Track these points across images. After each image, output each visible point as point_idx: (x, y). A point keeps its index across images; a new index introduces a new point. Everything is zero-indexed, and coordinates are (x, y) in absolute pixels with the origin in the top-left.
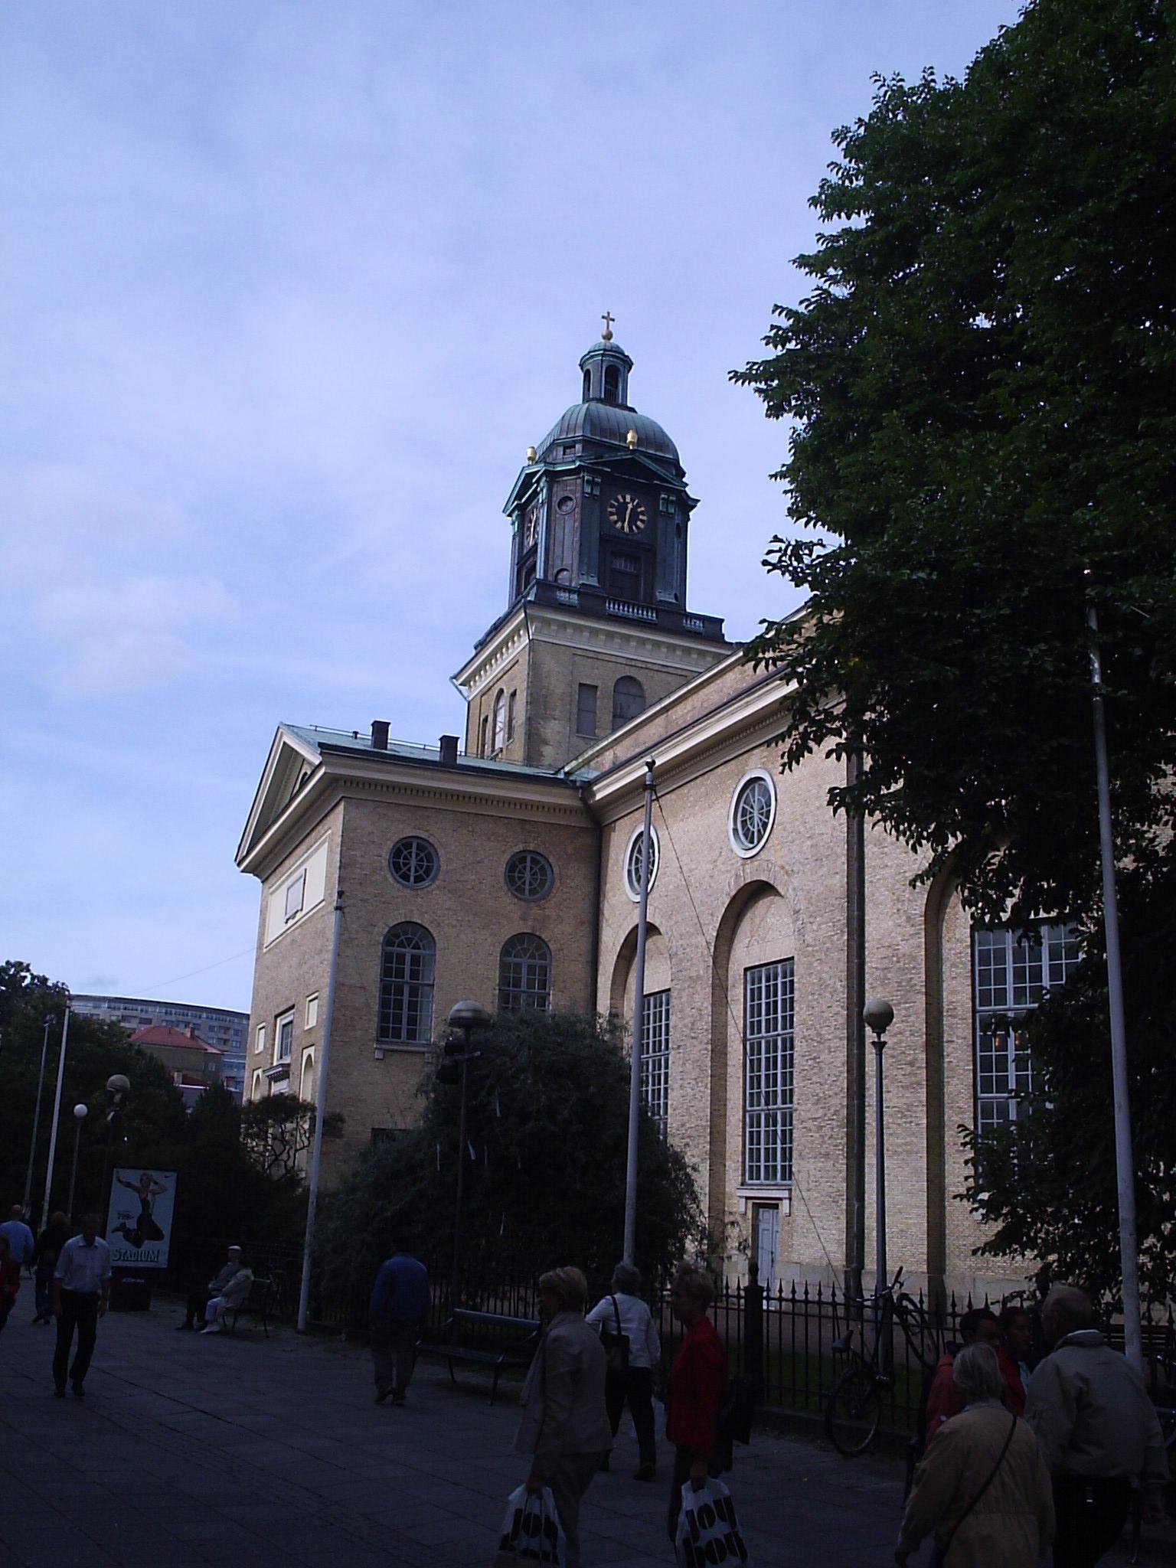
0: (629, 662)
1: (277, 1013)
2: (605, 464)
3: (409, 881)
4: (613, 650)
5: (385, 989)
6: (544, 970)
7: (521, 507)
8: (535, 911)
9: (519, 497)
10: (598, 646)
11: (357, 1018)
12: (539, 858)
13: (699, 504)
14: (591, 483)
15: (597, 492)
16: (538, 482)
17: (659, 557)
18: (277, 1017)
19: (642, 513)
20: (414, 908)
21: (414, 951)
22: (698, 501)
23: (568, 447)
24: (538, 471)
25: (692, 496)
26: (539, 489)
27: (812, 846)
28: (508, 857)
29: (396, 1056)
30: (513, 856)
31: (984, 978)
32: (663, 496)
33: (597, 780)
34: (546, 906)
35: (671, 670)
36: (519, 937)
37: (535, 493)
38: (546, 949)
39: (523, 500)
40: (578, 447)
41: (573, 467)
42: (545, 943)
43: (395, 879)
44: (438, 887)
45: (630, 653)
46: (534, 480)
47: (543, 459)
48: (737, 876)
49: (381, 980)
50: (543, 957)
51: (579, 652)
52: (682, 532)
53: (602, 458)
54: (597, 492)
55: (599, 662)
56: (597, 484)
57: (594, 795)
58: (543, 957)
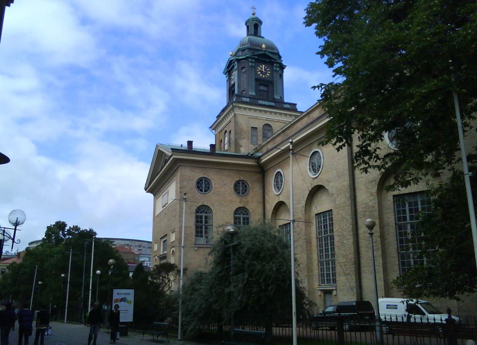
1: (161, 237)
2: (256, 55)
5: (197, 227)
6: (248, 219)
7: (229, 71)
8: (244, 200)
9: (228, 68)
10: (257, 114)
13: (286, 67)
15: (253, 65)
16: (234, 63)
17: (275, 84)
19: (268, 71)
21: (205, 214)
22: (286, 66)
23: (243, 50)
28: (234, 182)
29: (202, 249)
30: (235, 182)
31: (399, 212)
32: (275, 65)
34: (248, 197)
36: (239, 208)
37: (233, 67)
41: (245, 57)
42: (248, 210)
43: (198, 191)
44: (212, 193)
47: (235, 55)
48: (311, 184)
52: (281, 76)
53: (254, 53)
54: (253, 65)
56: (253, 62)
57: (261, 160)
58: (247, 214)
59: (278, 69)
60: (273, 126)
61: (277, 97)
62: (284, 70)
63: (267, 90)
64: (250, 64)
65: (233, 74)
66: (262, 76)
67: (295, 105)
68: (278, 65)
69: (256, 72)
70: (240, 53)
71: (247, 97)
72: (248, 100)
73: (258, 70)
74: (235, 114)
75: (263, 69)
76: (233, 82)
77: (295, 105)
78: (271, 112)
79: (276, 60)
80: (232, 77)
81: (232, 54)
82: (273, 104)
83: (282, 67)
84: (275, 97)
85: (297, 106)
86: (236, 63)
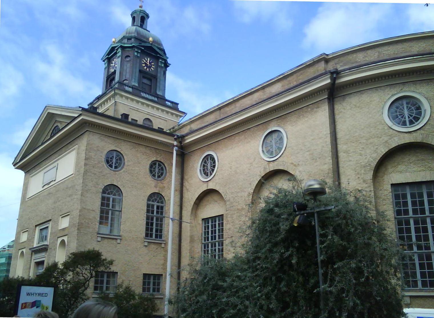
1: (36, 224)
3: (112, 168)
5: (102, 212)
6: (162, 208)
7: (109, 58)
9: (108, 54)
10: (139, 106)
11: (90, 223)
12: (161, 164)
13: (170, 66)
14: (137, 52)
15: (139, 55)
16: (117, 50)
17: (158, 80)
18: (36, 226)
19: (153, 65)
20: (115, 179)
21: (113, 196)
23: (129, 39)
24: (118, 46)
25: (169, 63)
26: (118, 52)
27: (310, 154)
28: (150, 162)
29: (106, 240)
30: (152, 162)
33: (187, 135)
34: (164, 182)
36: (154, 194)
37: (116, 53)
38: (163, 199)
39: (110, 56)
40: (133, 40)
41: (131, 46)
42: (163, 197)
43: (107, 166)
44: (124, 171)
45: (149, 110)
46: (116, 49)
47: (120, 41)
48: (265, 168)
49: (101, 208)
50: (162, 203)
51: (132, 108)
52: (165, 74)
53: (141, 44)
54: (139, 55)
55: (138, 112)
56: (139, 53)
57: (185, 140)
58: (162, 203)
59: (163, 65)
60: (153, 122)
61: (159, 93)
62: (168, 68)
63: (150, 84)
64: (136, 54)
65: (113, 62)
66: (147, 69)
68: (163, 62)
69: (141, 64)
70: (126, 41)
71: (129, 87)
72: (130, 90)
73: (143, 62)
74: (115, 102)
75: (147, 62)
76: (112, 70)
77: (178, 104)
78: (153, 107)
80: (112, 65)
81: (115, 40)
83: (166, 65)
84: (157, 92)
85: (179, 105)
86: (120, 50)
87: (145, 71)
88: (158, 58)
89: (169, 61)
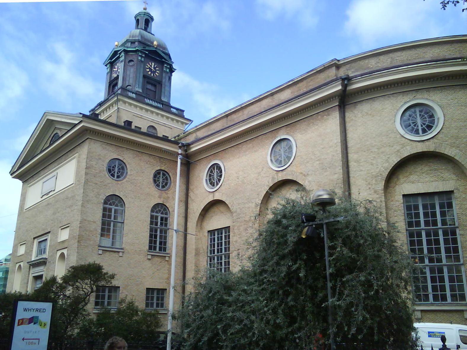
0: (152, 121)
3: (114, 177)
4: (149, 116)
5: (103, 224)
6: (166, 219)
7: (112, 62)
8: (164, 195)
9: (111, 59)
10: (143, 113)
11: (91, 235)
12: (165, 173)
13: (176, 71)
14: (141, 56)
15: (143, 60)
16: (120, 54)
17: (163, 86)
18: (34, 238)
19: (158, 70)
20: (117, 189)
21: (115, 207)
22: (176, 70)
23: (133, 42)
24: (121, 50)
25: (174, 67)
26: (121, 56)
27: (320, 163)
29: (108, 253)
32: (165, 65)
33: (193, 143)
34: (168, 193)
35: (167, 126)
37: (119, 57)
40: (136, 43)
41: (135, 50)
44: (127, 181)
45: (154, 117)
46: (119, 53)
47: (123, 45)
49: (102, 219)
50: (166, 214)
51: (136, 115)
52: (170, 79)
53: (145, 48)
54: (143, 60)
55: (142, 119)
56: (143, 57)
57: (190, 149)
58: (166, 214)
59: (168, 70)
61: (164, 99)
62: (173, 74)
63: (155, 90)
64: (140, 58)
65: (116, 67)
66: (151, 74)
67: (183, 111)
68: (168, 67)
69: (145, 69)
70: (129, 44)
71: (133, 93)
72: (134, 96)
73: (147, 67)
74: (118, 108)
76: (115, 75)
77: (183, 111)
78: (158, 114)
79: (168, 61)
80: (114, 70)
81: (118, 44)
82: (160, 106)
83: (172, 70)
84: (162, 99)
85: (184, 112)
86: (123, 54)
87: (150, 76)
88: (162, 63)
89: (174, 66)
